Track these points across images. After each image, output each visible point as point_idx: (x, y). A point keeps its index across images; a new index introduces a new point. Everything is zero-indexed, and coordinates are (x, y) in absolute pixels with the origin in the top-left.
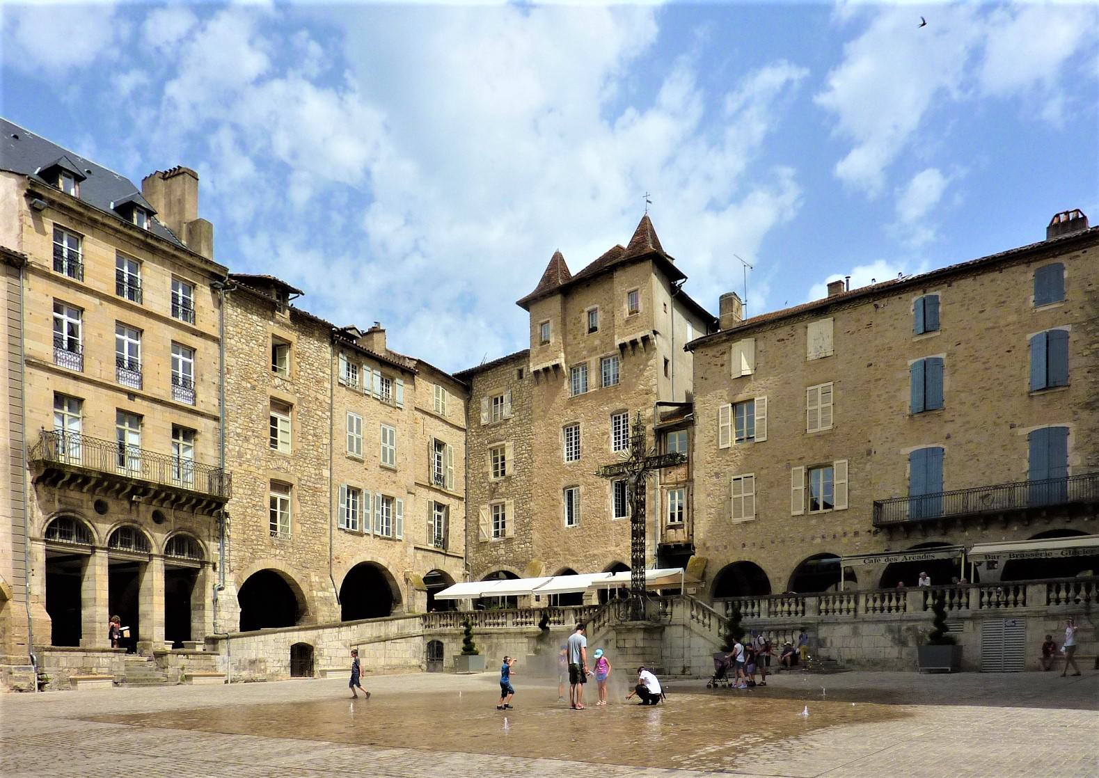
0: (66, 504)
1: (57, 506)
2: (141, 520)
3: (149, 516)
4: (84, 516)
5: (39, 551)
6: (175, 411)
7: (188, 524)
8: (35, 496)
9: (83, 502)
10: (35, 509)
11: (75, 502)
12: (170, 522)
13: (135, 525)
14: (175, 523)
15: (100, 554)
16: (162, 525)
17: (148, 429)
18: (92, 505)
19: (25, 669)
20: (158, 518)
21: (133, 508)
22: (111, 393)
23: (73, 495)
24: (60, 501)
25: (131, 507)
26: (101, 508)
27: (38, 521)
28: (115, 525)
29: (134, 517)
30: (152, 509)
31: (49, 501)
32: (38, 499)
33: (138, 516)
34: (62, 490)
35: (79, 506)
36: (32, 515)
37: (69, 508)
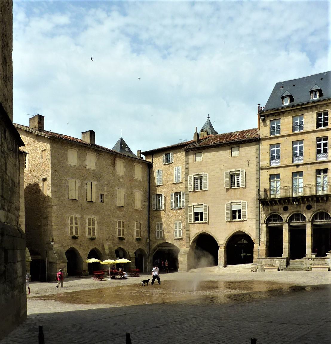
0: (273, 210)
1: (270, 212)
2: (301, 210)
3: (305, 208)
4: (278, 213)
5: (264, 227)
6: (317, 165)
7: (323, 207)
8: (263, 210)
9: (279, 209)
10: (263, 214)
11: (276, 209)
12: (314, 208)
13: (299, 212)
14: (316, 208)
15: (285, 225)
16: (311, 210)
17: (305, 175)
18: (282, 209)
19: (255, 265)
20: (309, 208)
21: (298, 206)
22: (289, 168)
23: (276, 207)
24: (271, 210)
25: (297, 206)
26: (286, 209)
27: (264, 217)
28: (290, 214)
29: (298, 209)
30: (306, 205)
31: (267, 211)
32: (264, 211)
33: (300, 209)
34: (272, 206)
35: (277, 210)
36: (262, 216)
37: (274, 211)
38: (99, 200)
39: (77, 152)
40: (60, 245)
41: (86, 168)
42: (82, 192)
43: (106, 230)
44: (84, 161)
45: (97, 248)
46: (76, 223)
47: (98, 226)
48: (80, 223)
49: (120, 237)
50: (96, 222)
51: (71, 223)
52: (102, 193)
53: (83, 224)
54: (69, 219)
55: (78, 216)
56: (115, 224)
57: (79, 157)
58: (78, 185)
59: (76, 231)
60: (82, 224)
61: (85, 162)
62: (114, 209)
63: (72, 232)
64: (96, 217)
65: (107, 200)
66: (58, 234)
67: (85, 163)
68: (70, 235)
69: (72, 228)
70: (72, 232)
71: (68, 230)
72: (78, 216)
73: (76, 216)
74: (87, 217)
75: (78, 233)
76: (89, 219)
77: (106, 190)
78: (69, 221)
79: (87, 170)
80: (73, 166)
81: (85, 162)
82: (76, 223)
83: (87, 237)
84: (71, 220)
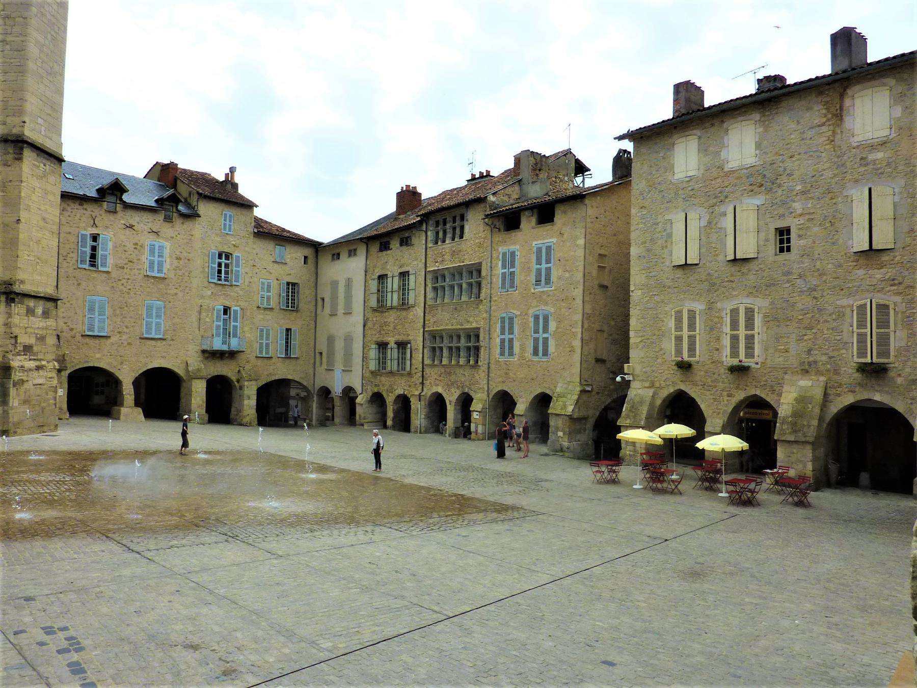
38: (772, 247)
39: (700, 138)
40: (647, 384)
41: (726, 170)
42: (714, 237)
43: (800, 339)
44: (718, 154)
45: (763, 396)
46: (692, 327)
47: (765, 328)
48: (703, 327)
49: (863, 360)
50: (761, 315)
51: (679, 328)
52: (782, 224)
53: (713, 328)
54: (673, 317)
55: (699, 307)
56: (841, 315)
57: (703, 150)
58: (704, 223)
59: (692, 350)
60: (712, 329)
61: (722, 153)
62: (840, 266)
63: (679, 351)
64: (760, 304)
65: (802, 242)
66: (643, 358)
67: (722, 158)
68: (673, 358)
69: (679, 339)
70: (679, 351)
71: (669, 346)
72: (699, 307)
73: (691, 308)
74: (729, 306)
75: (698, 353)
76: (734, 312)
77: (799, 212)
78: (672, 324)
79: (733, 172)
80: (687, 179)
81: (723, 154)
82: (692, 327)
83: (725, 364)
84: (679, 319)
